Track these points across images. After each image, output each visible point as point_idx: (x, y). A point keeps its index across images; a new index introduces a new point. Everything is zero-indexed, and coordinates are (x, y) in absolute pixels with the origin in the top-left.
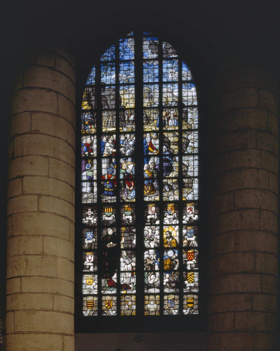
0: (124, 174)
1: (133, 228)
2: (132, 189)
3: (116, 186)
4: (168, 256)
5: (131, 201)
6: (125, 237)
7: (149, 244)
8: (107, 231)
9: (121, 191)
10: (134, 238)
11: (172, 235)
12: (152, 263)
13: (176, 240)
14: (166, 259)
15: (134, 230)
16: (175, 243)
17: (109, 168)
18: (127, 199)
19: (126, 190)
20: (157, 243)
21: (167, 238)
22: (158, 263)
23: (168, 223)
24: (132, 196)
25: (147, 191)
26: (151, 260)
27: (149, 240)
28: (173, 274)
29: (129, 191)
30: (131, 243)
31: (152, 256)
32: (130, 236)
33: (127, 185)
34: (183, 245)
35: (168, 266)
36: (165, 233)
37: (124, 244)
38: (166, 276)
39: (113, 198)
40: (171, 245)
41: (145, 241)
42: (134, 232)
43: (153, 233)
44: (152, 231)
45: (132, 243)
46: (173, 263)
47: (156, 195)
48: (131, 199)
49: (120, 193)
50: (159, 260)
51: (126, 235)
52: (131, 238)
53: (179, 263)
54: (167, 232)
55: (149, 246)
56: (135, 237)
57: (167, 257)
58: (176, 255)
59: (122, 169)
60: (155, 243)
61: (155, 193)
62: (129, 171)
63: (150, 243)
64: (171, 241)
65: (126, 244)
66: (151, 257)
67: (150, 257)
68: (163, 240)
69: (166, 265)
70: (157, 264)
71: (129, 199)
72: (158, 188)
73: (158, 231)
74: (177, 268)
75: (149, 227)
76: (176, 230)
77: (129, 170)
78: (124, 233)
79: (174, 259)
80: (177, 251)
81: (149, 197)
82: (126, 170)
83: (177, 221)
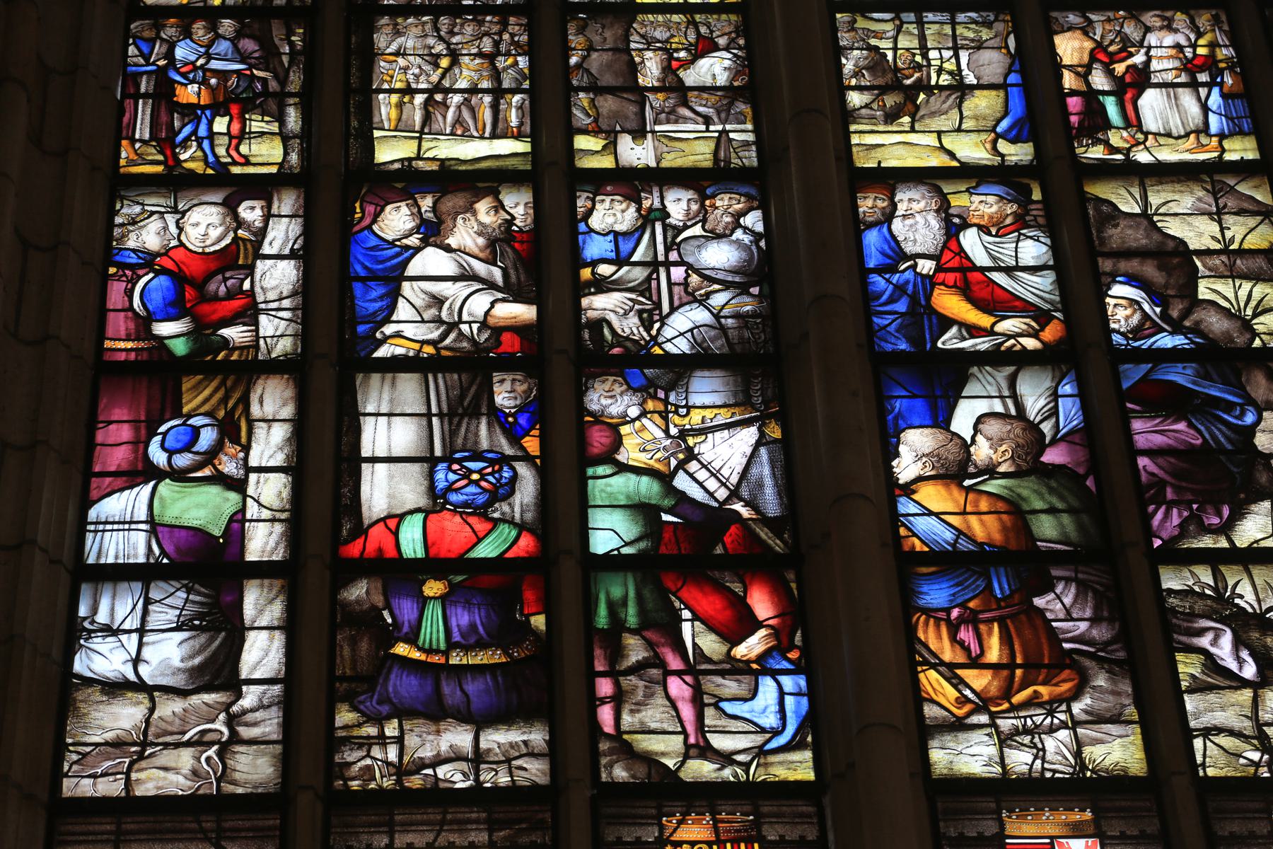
0: (642, 510)
2: (761, 658)
3: (539, 621)
5: (757, 774)
9: (613, 674)
17: (448, 459)
18: (706, 751)
19: (675, 663)
24: (770, 720)
25: (967, 674)
29: (723, 673)
33: (686, 614)
39: (496, 739)
47: (1097, 719)
48: (761, 752)
49: (605, 687)
59: (623, 468)
61: (1076, 695)
62: (712, 484)
71: (726, 758)
72: (1105, 645)
77: (702, 475)
81: (1005, 740)
82: (665, 479)
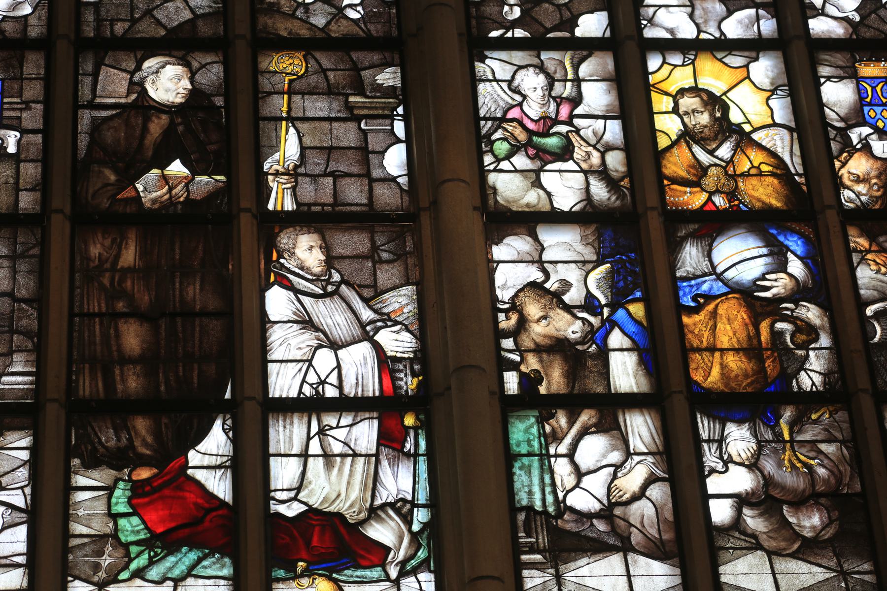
1: (376, 57)
4: (719, 277)
6: (304, 127)
7: (537, 184)
8: (132, 74)
10: (392, 131)
11: (735, 117)
12: (572, 329)
13: (773, 154)
14: (709, 298)
15: (388, 77)
16: (769, 180)
20: (603, 173)
21: (688, 136)
22: (631, 328)
23: (687, 31)
26: (568, 309)
27: (531, 152)
28: (792, 425)
30: (368, 174)
31: (573, 274)
32: (358, 119)
34: (847, 194)
35: (734, 362)
36: (662, 103)
37: (294, 174)
38: (721, 441)
40: (732, 195)
41: (498, 160)
42: (390, 91)
43: (559, 101)
44: (551, 86)
45: (376, 173)
46: (781, 333)
50: (637, 310)
51: (318, 107)
52: (365, 133)
53: (835, 334)
54: (682, 92)
55: (532, 197)
56: (399, 128)
57: (707, 285)
58: (796, 267)
60: (585, 172)
63: (538, 172)
64: (731, 161)
65: (314, 177)
66: (566, 285)
67: (552, 285)
68: (659, 155)
69: (712, 349)
70: (626, 343)
73: (602, 85)
74: (818, 379)
75: (519, 57)
76: (768, 86)
78: (291, 92)
79: (777, 300)
80: (795, 244)
83: (758, 19)
